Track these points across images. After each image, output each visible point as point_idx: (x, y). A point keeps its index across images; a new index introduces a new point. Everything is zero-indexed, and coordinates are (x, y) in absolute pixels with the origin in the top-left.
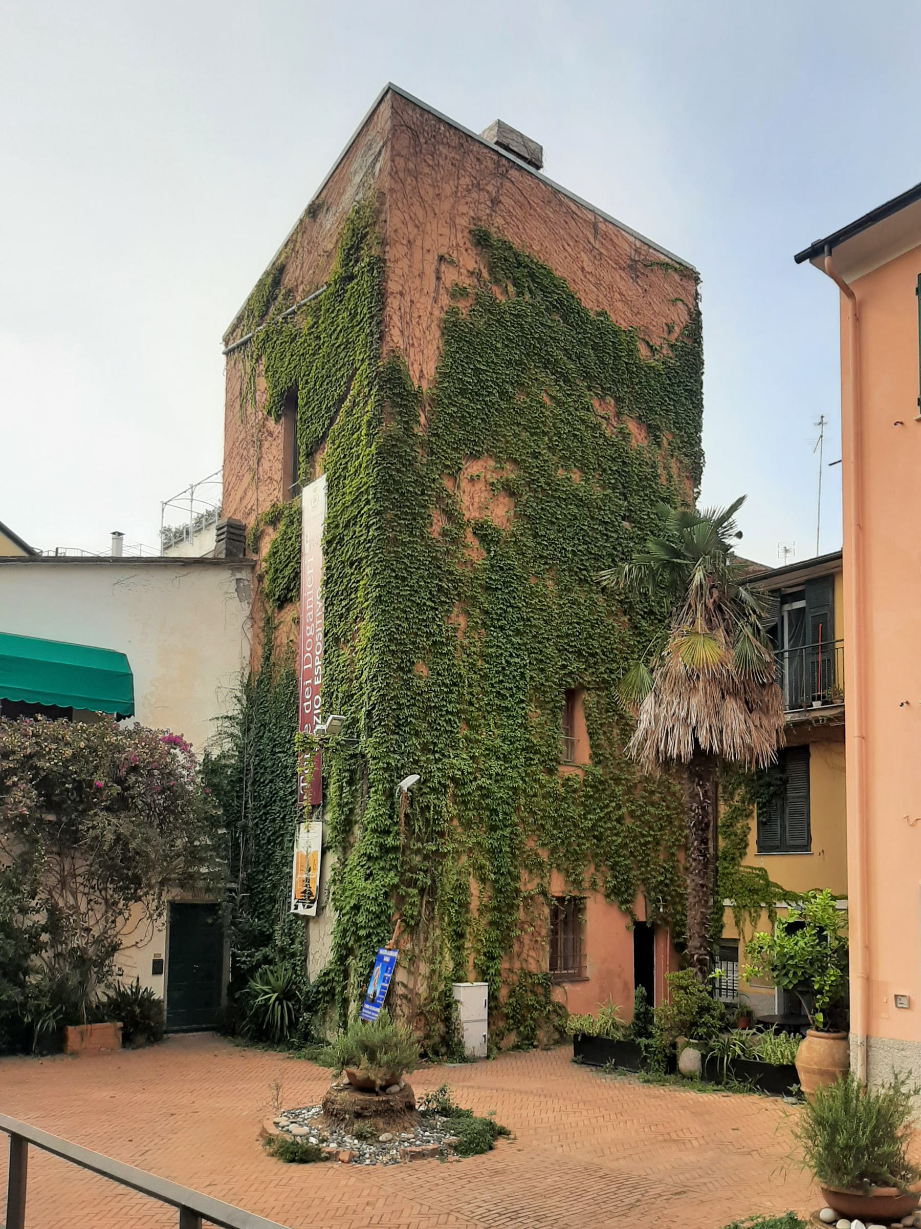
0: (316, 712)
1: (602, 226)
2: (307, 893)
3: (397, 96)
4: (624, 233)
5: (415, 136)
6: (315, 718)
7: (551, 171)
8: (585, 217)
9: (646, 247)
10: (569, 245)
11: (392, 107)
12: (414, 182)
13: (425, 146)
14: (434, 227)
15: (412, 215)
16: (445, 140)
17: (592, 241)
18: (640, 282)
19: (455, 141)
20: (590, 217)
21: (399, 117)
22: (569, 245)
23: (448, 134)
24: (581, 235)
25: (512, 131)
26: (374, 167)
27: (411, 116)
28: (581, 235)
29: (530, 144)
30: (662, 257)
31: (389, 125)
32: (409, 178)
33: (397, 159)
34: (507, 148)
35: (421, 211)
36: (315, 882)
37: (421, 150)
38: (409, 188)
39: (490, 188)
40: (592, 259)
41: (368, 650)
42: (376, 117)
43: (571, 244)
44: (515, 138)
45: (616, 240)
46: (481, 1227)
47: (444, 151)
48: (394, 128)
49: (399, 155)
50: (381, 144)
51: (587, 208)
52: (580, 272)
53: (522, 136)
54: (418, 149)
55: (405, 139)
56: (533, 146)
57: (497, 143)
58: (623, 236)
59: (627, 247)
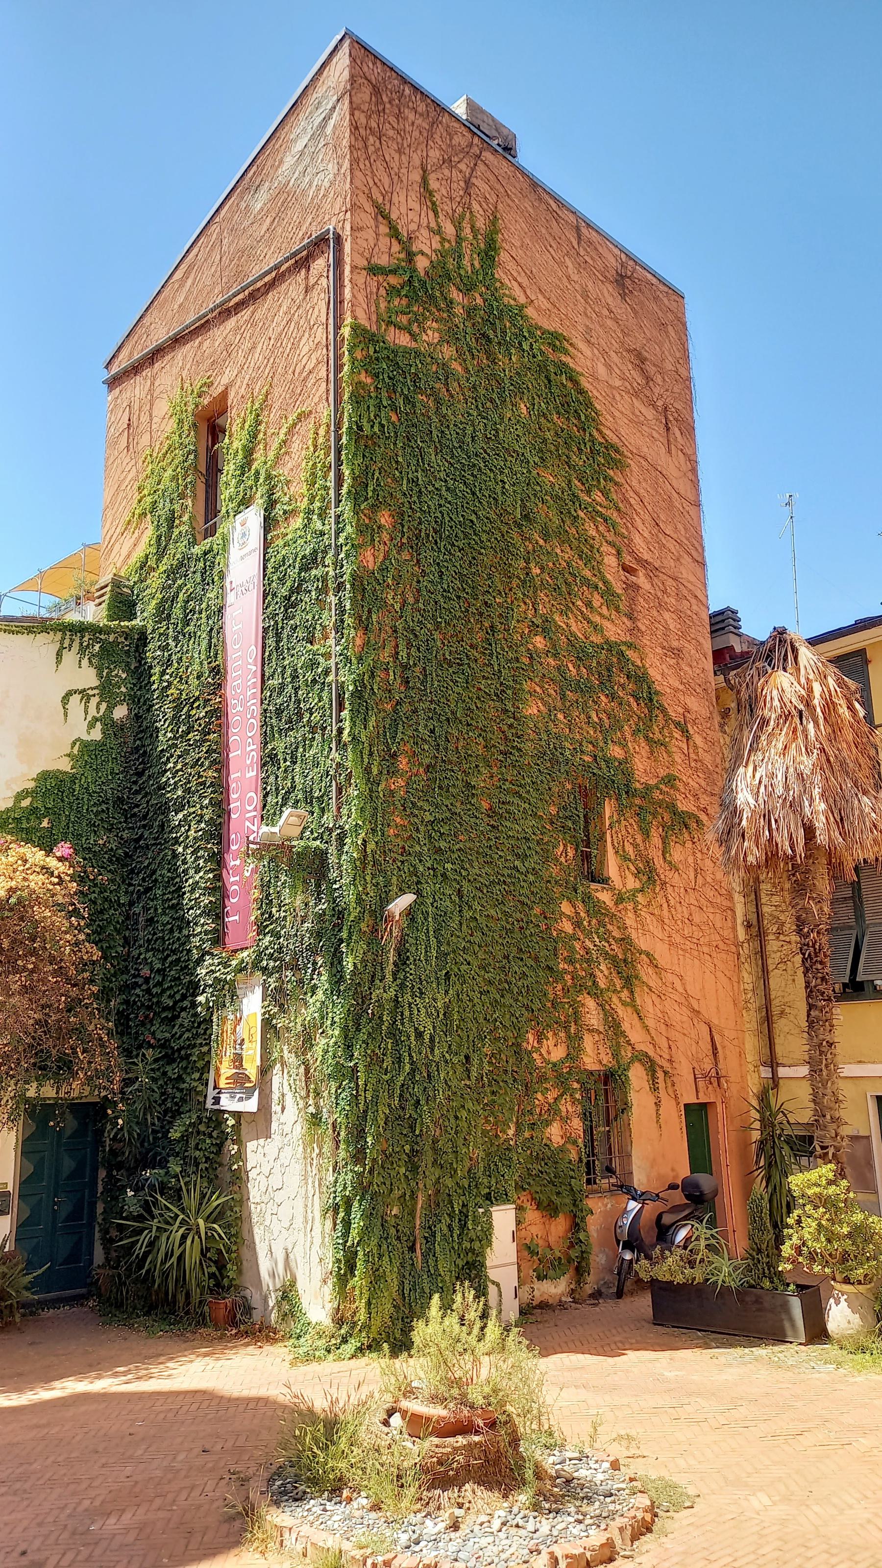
0: (248, 815)
1: (584, 231)
2: (240, 1079)
3: (356, 45)
4: (608, 243)
5: (376, 91)
6: (247, 823)
7: (526, 157)
8: (566, 218)
9: (631, 263)
10: (551, 246)
11: (350, 55)
12: (378, 142)
13: (388, 106)
14: (402, 198)
15: (376, 180)
16: (411, 104)
17: (576, 247)
18: (627, 299)
19: (422, 108)
20: (572, 218)
21: (357, 68)
22: (551, 246)
23: (414, 98)
24: (563, 237)
25: (483, 112)
26: (325, 127)
27: (374, 72)
28: (563, 237)
29: (503, 129)
30: (649, 276)
31: (346, 75)
32: (371, 138)
33: (357, 113)
34: (478, 128)
35: (386, 177)
36: (253, 1060)
37: (384, 110)
38: (371, 149)
39: (462, 166)
40: (577, 266)
41: (558, 283)
42: (325, 73)
43: (554, 246)
44: (486, 119)
45: (600, 250)
46: (541, 1563)
47: (412, 117)
48: (352, 79)
49: (359, 109)
50: (335, 98)
51: (568, 210)
52: (565, 280)
53: (493, 119)
54: (381, 108)
55: (365, 94)
56: (505, 132)
57: (467, 120)
58: (607, 247)
59: (613, 260)
